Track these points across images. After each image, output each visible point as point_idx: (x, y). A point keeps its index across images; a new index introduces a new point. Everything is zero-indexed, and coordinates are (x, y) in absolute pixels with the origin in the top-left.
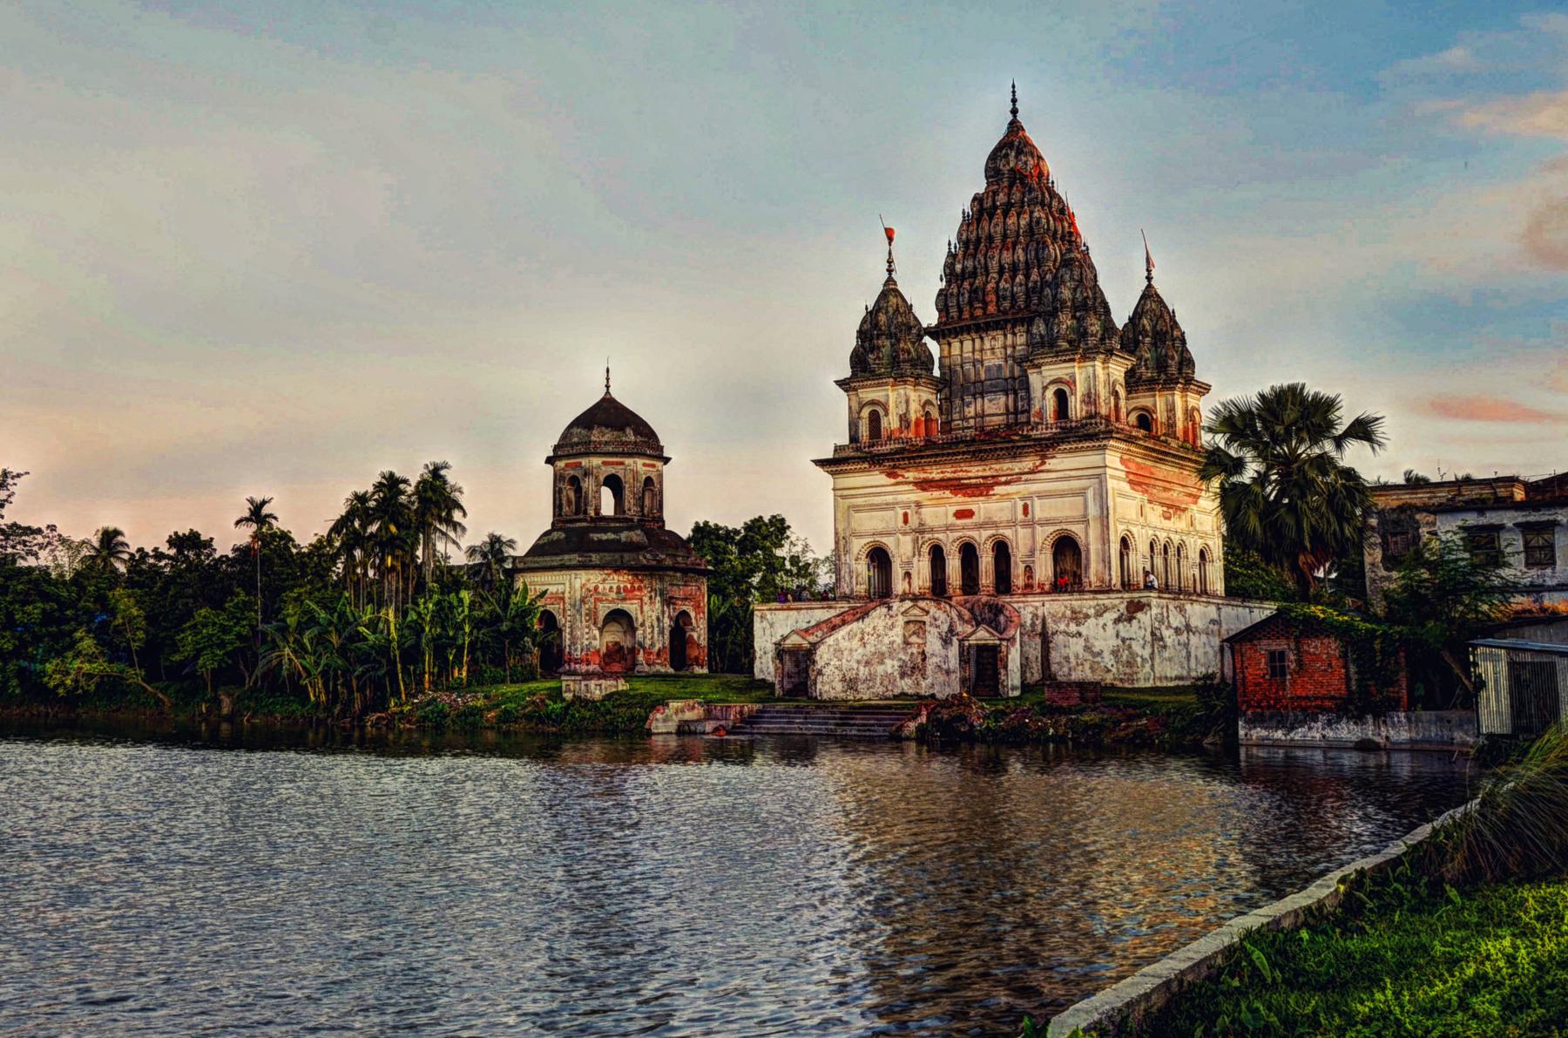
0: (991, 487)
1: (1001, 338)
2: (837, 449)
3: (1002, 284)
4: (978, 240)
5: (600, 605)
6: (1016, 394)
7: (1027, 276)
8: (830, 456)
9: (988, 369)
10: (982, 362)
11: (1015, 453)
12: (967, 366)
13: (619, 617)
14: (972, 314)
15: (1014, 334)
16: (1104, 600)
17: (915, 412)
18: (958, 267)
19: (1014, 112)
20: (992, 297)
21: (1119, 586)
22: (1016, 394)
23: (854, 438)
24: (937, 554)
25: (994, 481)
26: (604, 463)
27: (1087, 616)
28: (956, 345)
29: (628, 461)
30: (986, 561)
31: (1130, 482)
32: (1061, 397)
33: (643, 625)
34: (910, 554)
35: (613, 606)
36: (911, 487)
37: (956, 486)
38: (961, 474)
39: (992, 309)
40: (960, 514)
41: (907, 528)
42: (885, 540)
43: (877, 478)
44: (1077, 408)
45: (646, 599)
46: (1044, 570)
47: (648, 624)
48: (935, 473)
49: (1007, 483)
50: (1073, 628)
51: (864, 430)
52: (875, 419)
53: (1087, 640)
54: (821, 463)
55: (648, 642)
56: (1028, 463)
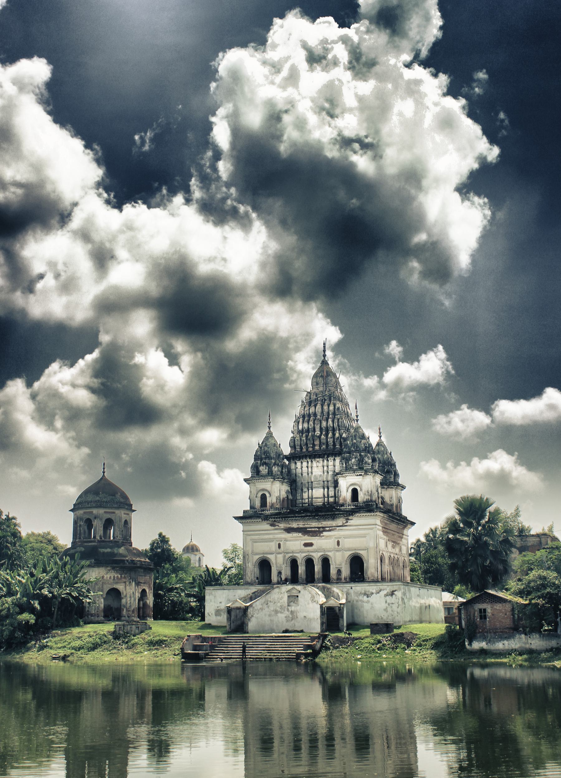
0: (322, 532)
1: (321, 462)
2: (244, 512)
3: (323, 437)
4: (309, 416)
5: (105, 586)
6: (328, 489)
7: (334, 435)
8: (241, 515)
9: (315, 476)
10: (312, 473)
11: (333, 517)
12: (305, 474)
13: (115, 593)
14: (307, 450)
15: (328, 460)
16: (380, 586)
17: (284, 495)
18: (300, 427)
19: (324, 356)
20: (317, 442)
21: (380, 580)
22: (328, 489)
23: (252, 507)
24: (294, 563)
25: (324, 529)
26: (105, 512)
27: (372, 593)
28: (299, 464)
29: (117, 512)
30: (318, 568)
31: (383, 532)
32: (355, 492)
33: (126, 596)
34: (282, 563)
35: (111, 587)
36: (282, 531)
37: (304, 531)
38: (307, 526)
39: (317, 448)
40: (306, 545)
41: (280, 551)
42: (269, 556)
43: (265, 526)
44: (362, 497)
45: (127, 583)
46: (346, 572)
47: (128, 596)
48: (295, 525)
49: (330, 531)
50: (365, 598)
51: (258, 503)
52: (264, 497)
53: (372, 604)
54: (236, 518)
55: (128, 605)
56: (340, 521)
